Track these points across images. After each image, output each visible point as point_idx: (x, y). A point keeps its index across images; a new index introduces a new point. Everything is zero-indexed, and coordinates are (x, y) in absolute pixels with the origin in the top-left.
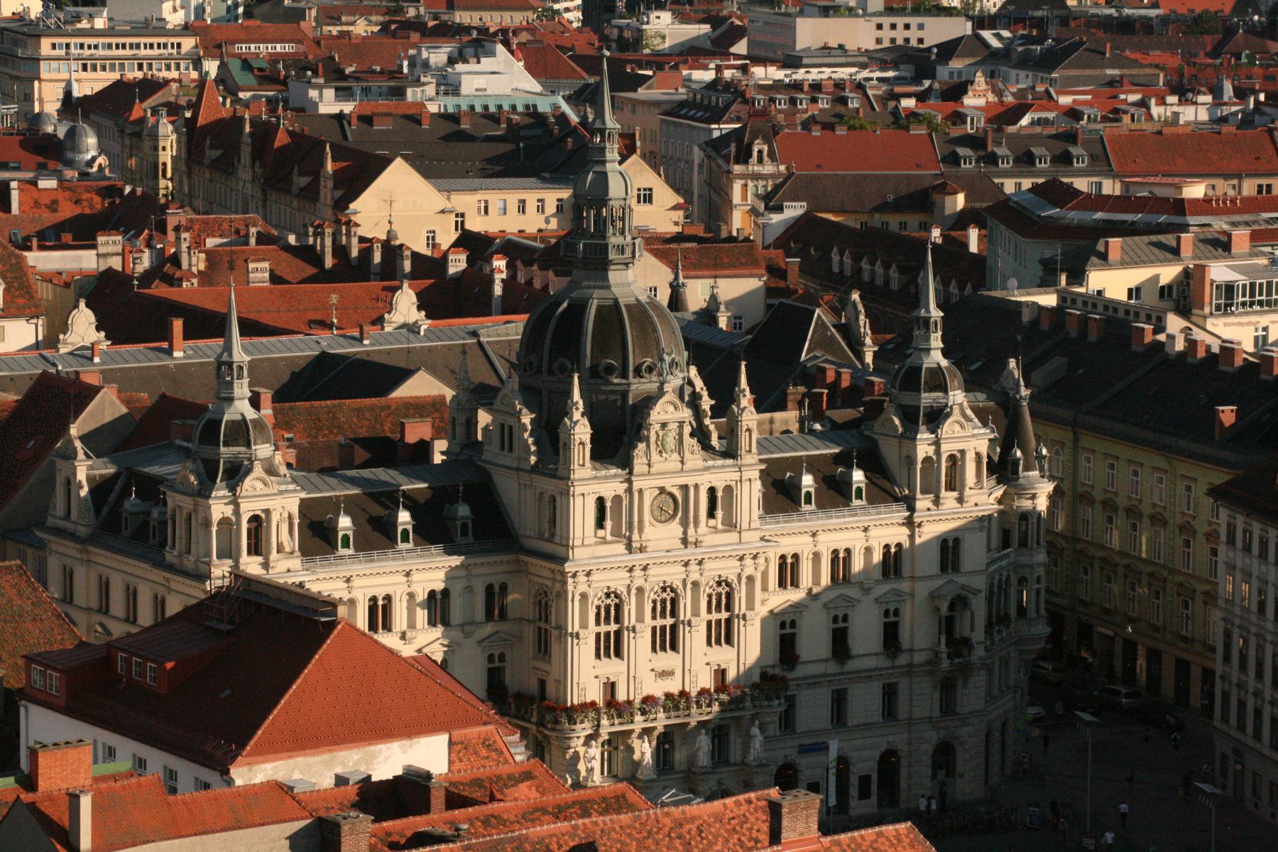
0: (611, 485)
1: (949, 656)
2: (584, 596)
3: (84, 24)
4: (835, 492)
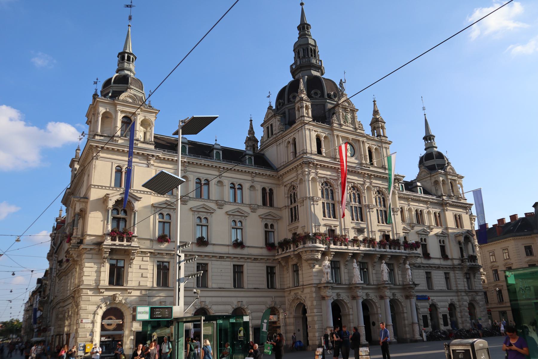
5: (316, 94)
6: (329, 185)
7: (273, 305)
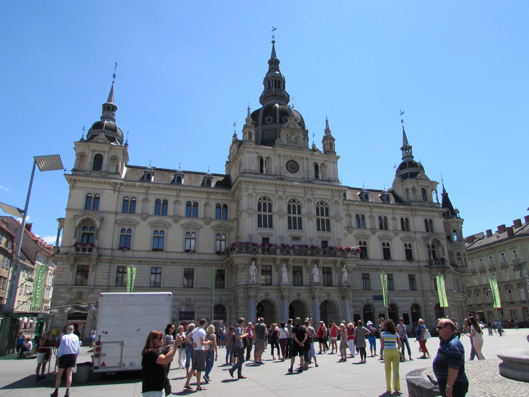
0: (266, 151)
5: (269, 120)
6: (267, 199)
7: (219, 303)
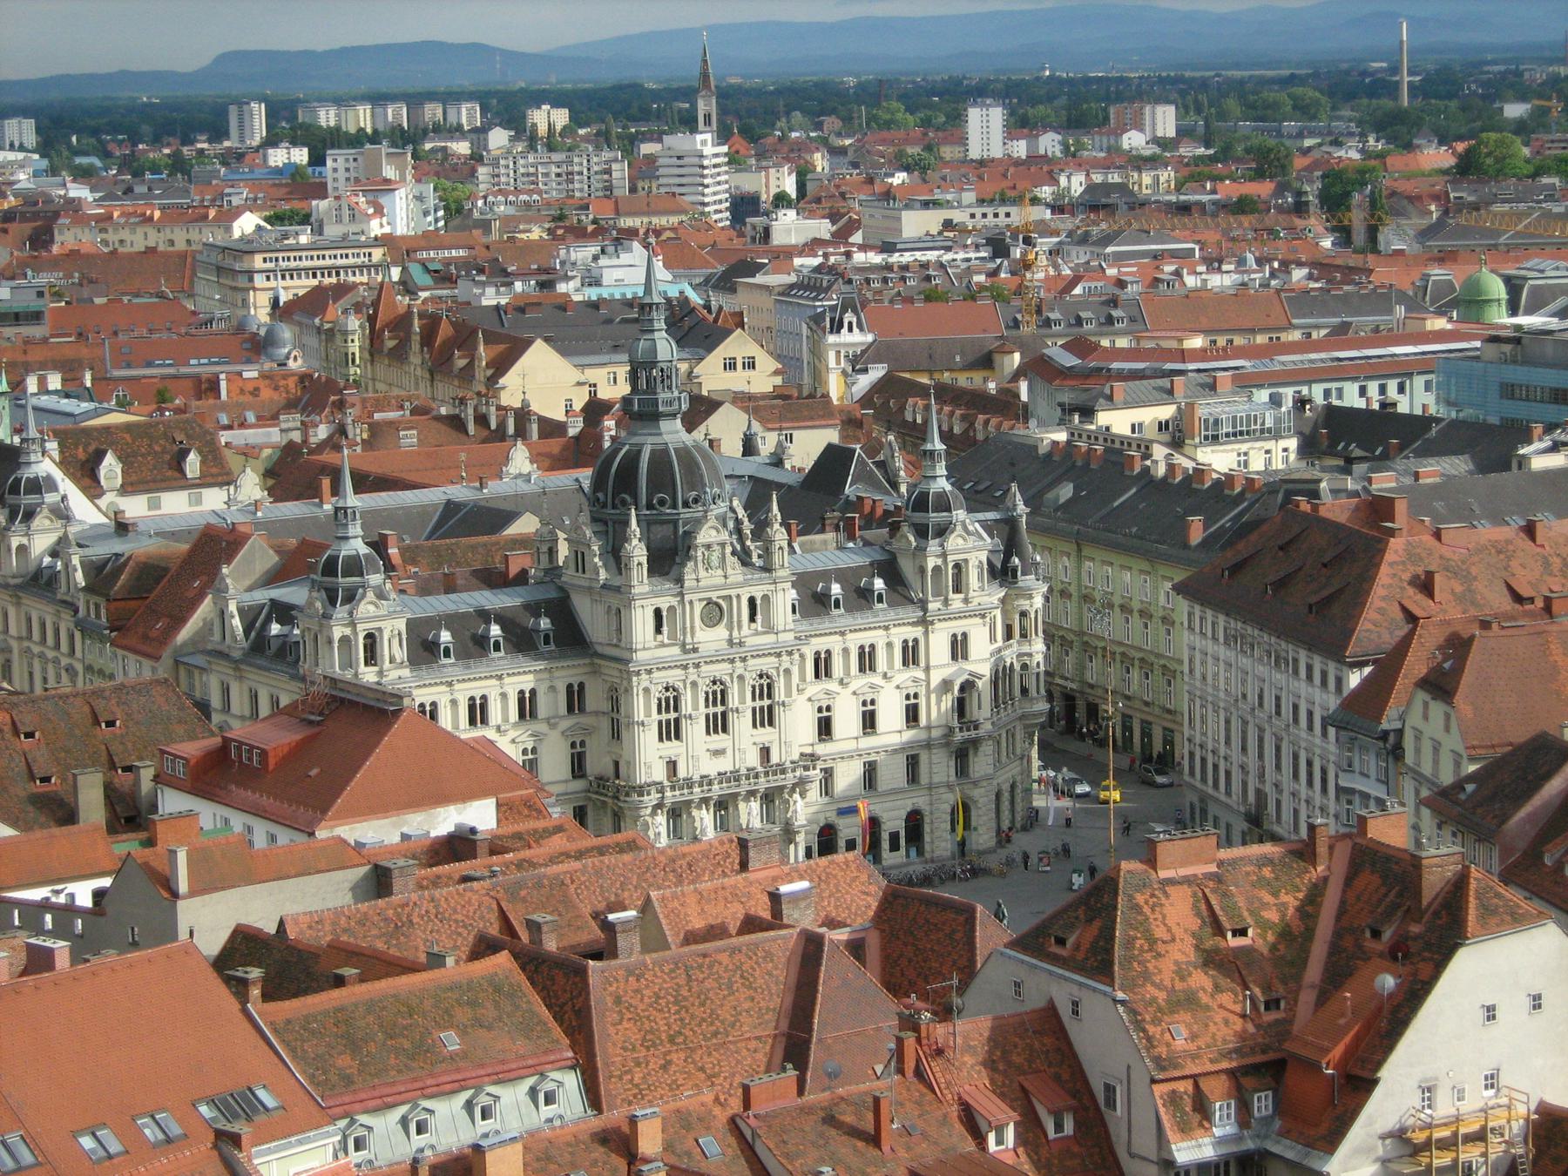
1: (961, 729)
2: (646, 690)
3: (291, 241)
4: (862, 597)
